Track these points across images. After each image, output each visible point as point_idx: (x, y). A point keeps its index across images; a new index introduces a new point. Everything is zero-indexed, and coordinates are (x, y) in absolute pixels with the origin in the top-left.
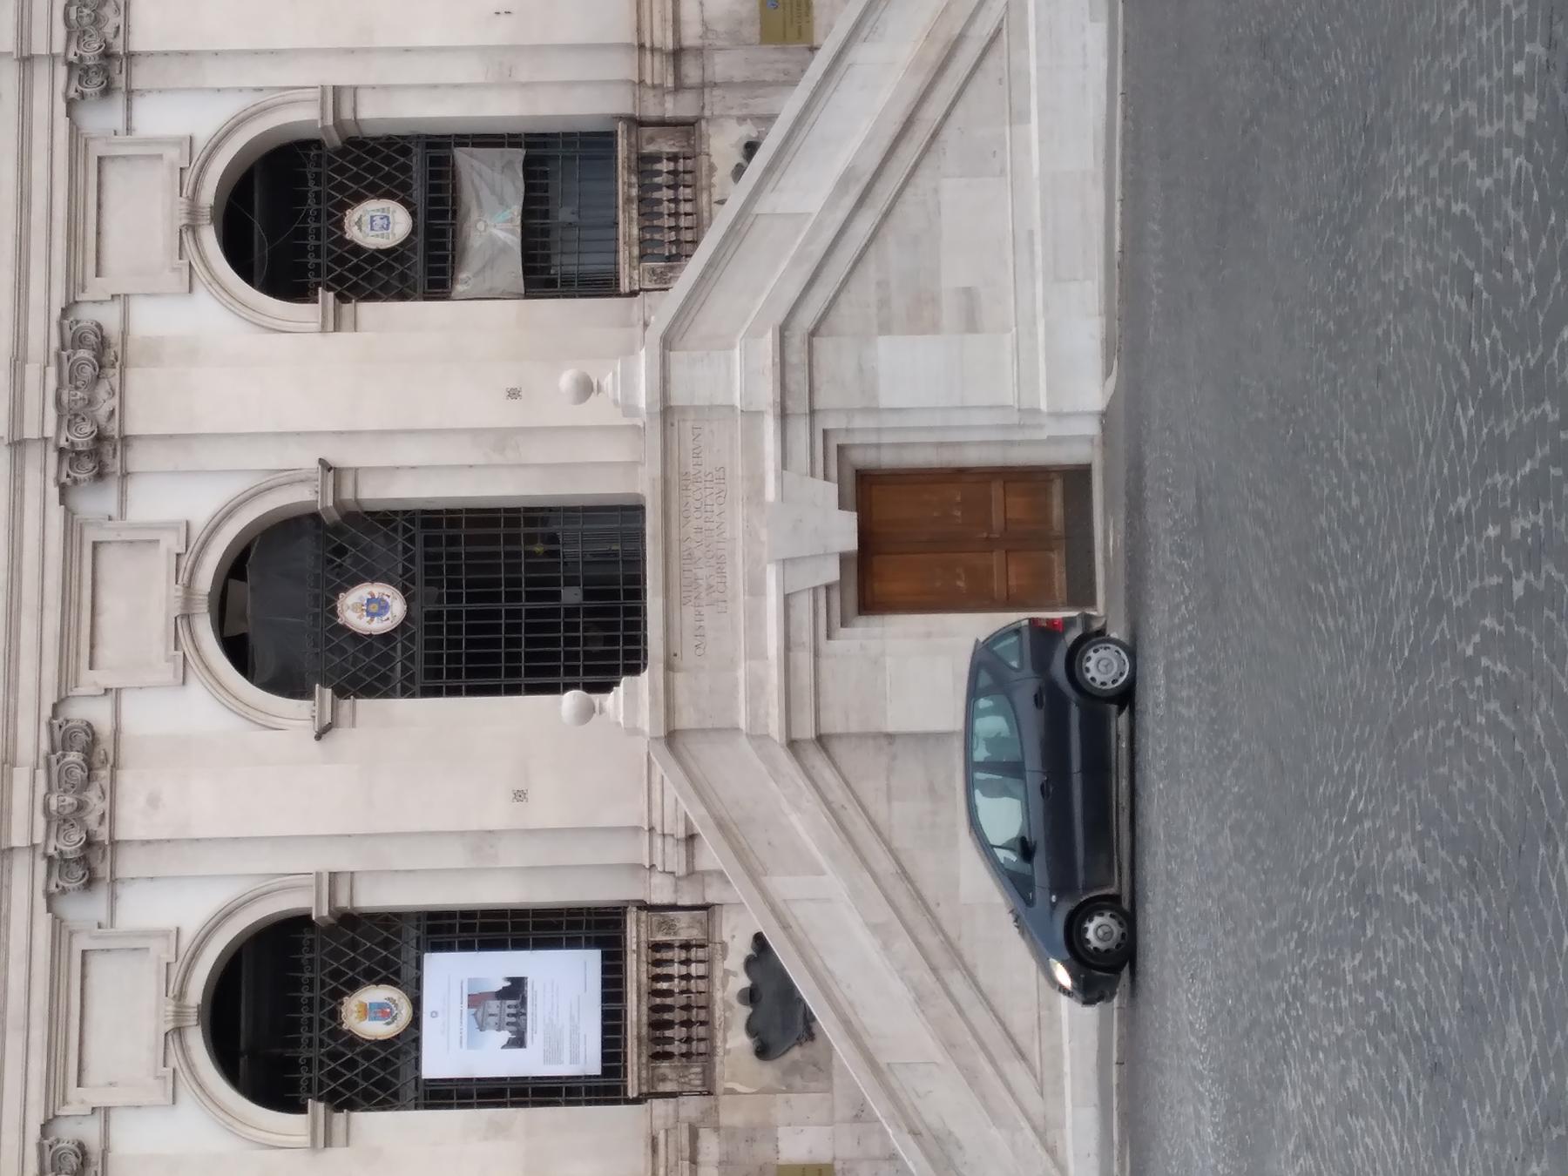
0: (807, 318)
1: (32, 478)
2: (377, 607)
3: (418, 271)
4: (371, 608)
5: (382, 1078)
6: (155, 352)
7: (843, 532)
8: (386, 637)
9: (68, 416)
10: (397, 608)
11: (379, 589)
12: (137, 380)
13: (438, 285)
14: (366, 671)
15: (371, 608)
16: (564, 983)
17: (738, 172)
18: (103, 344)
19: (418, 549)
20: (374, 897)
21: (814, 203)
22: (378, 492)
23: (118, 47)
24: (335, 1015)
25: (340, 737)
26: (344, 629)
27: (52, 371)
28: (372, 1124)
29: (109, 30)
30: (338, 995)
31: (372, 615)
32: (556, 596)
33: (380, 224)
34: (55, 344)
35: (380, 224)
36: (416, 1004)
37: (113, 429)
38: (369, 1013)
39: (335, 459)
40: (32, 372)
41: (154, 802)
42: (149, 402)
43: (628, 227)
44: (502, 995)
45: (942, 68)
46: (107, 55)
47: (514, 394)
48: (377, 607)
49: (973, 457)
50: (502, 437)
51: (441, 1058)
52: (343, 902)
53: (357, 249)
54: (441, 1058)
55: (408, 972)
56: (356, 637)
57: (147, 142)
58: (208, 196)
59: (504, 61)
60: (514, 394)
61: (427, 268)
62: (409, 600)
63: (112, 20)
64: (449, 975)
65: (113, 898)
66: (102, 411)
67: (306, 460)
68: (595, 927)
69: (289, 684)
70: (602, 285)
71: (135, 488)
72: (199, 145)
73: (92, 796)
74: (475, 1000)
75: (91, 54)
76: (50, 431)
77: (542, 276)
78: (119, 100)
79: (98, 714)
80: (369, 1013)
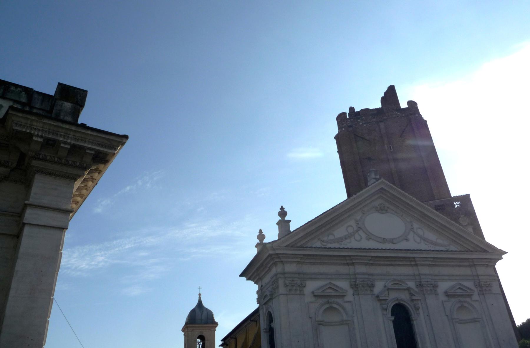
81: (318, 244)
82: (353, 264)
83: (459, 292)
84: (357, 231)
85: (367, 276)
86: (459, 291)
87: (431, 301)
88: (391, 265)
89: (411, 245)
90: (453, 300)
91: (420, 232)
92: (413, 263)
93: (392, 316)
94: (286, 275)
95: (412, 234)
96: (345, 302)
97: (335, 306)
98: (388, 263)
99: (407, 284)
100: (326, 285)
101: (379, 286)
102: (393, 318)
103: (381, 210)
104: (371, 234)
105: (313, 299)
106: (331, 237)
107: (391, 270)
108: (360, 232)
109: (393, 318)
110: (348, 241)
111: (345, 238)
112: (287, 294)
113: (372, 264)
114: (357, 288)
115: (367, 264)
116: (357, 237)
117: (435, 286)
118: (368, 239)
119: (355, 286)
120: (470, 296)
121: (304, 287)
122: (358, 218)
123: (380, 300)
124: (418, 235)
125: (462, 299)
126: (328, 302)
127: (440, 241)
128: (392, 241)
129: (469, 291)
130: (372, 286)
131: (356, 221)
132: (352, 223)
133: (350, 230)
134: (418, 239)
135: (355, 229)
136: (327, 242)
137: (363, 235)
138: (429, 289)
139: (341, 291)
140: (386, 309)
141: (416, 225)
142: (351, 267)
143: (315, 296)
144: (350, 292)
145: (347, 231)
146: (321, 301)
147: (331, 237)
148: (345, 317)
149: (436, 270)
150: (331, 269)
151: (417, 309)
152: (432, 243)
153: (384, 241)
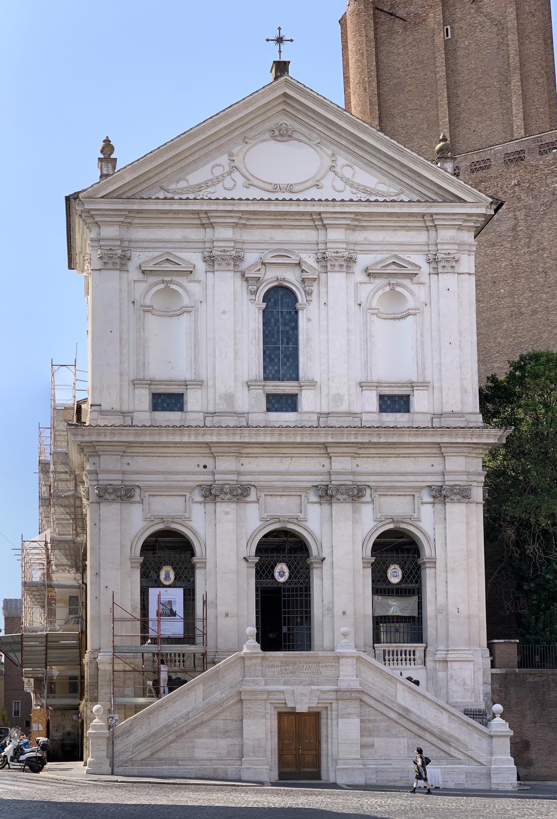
0: (366, 698)
1: (320, 478)
2: (282, 574)
3: (379, 586)
4: (282, 573)
5: (149, 578)
6: (355, 511)
7: (302, 708)
8: (273, 576)
9: (338, 488)
10: (282, 580)
11: (287, 574)
12: (348, 507)
13: (376, 591)
14: (263, 571)
15: (282, 573)
16: (174, 627)
17: (410, 679)
18: (359, 497)
19: (299, 585)
20: (199, 575)
21: (400, 700)
22: (316, 576)
23: (447, 500)
24: (166, 564)
25: (244, 564)
26: (276, 565)
27: (351, 483)
28: (137, 574)
29: (453, 497)
30: (172, 564)
31: (279, 573)
32: (285, 625)
33: (395, 575)
34: (359, 484)
35: (395, 575)
36: (169, 586)
37: (334, 500)
38: (167, 573)
39: (325, 562)
40: (350, 477)
41: (227, 513)
42: (342, 510)
43: (393, 646)
44: (171, 610)
45: (441, 739)
46: (445, 497)
47: (344, 613)
48: (282, 574)
49: (324, 746)
50: (331, 610)
51: (153, 592)
52: (198, 565)
53: (387, 568)
54: (153, 592)
55: (178, 584)
56: (273, 568)
57: (419, 508)
58: (403, 526)
59: (442, 610)
60: (344, 613)
61: (381, 587)
62: (284, 583)
63: (456, 498)
64: (176, 595)
65: (200, 503)
66: (340, 497)
67: (325, 554)
68: (189, 637)
69: (261, 549)
70: (377, 639)
71: (317, 506)
72: (418, 523)
73: (229, 496)
74: (170, 602)
75: (444, 493)
76: (333, 483)
77: (378, 621)
78: (431, 500)
79: (253, 496)
80: (167, 573)
81: (161, 195)
82: (212, 226)
83: (393, 269)
84: (230, 173)
85: (232, 244)
86: (394, 267)
87: (337, 281)
88: (280, 227)
89: (327, 193)
90: (379, 282)
91: (347, 173)
92: (317, 223)
93: (263, 302)
94: (102, 243)
95: (332, 174)
96: (189, 282)
97: (172, 286)
98: (274, 223)
99: (298, 256)
100: (161, 255)
101: (251, 258)
102: (264, 305)
103: (282, 135)
104: (254, 177)
105: (140, 276)
106: (182, 184)
107: (280, 235)
108: (236, 175)
109: (264, 305)
110: (210, 189)
111: (207, 184)
112: (100, 270)
113: (244, 224)
114: (213, 261)
115: (235, 225)
116: (228, 182)
117: (351, 260)
118: (249, 185)
119: (210, 260)
120: (411, 276)
121: (129, 259)
122: (234, 151)
123: (247, 280)
124: (342, 178)
125: (393, 281)
126: (163, 282)
127: (383, 188)
128: (290, 188)
129: (410, 267)
130: (238, 259)
131: (231, 155)
132: (224, 160)
133: (218, 172)
134: (340, 185)
135: (227, 169)
136: (175, 192)
137: (240, 180)
138: (337, 263)
139: (183, 265)
140: (255, 293)
141: (341, 161)
142: (209, 230)
143: (144, 272)
144: (201, 266)
145: (212, 173)
146: (152, 279)
147: (182, 184)
148: (186, 301)
149: (359, 236)
150: (177, 234)
151: (308, 294)
152: (365, 190)
153: (277, 188)
